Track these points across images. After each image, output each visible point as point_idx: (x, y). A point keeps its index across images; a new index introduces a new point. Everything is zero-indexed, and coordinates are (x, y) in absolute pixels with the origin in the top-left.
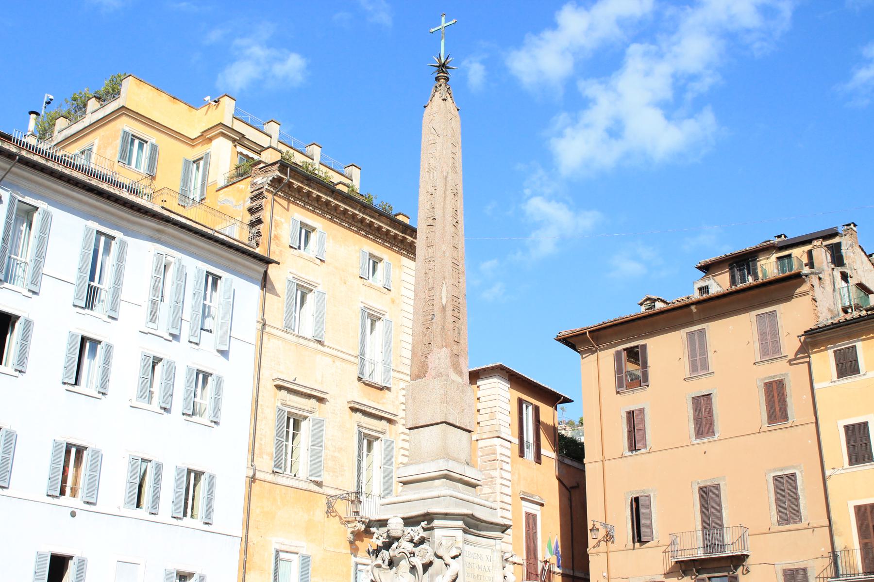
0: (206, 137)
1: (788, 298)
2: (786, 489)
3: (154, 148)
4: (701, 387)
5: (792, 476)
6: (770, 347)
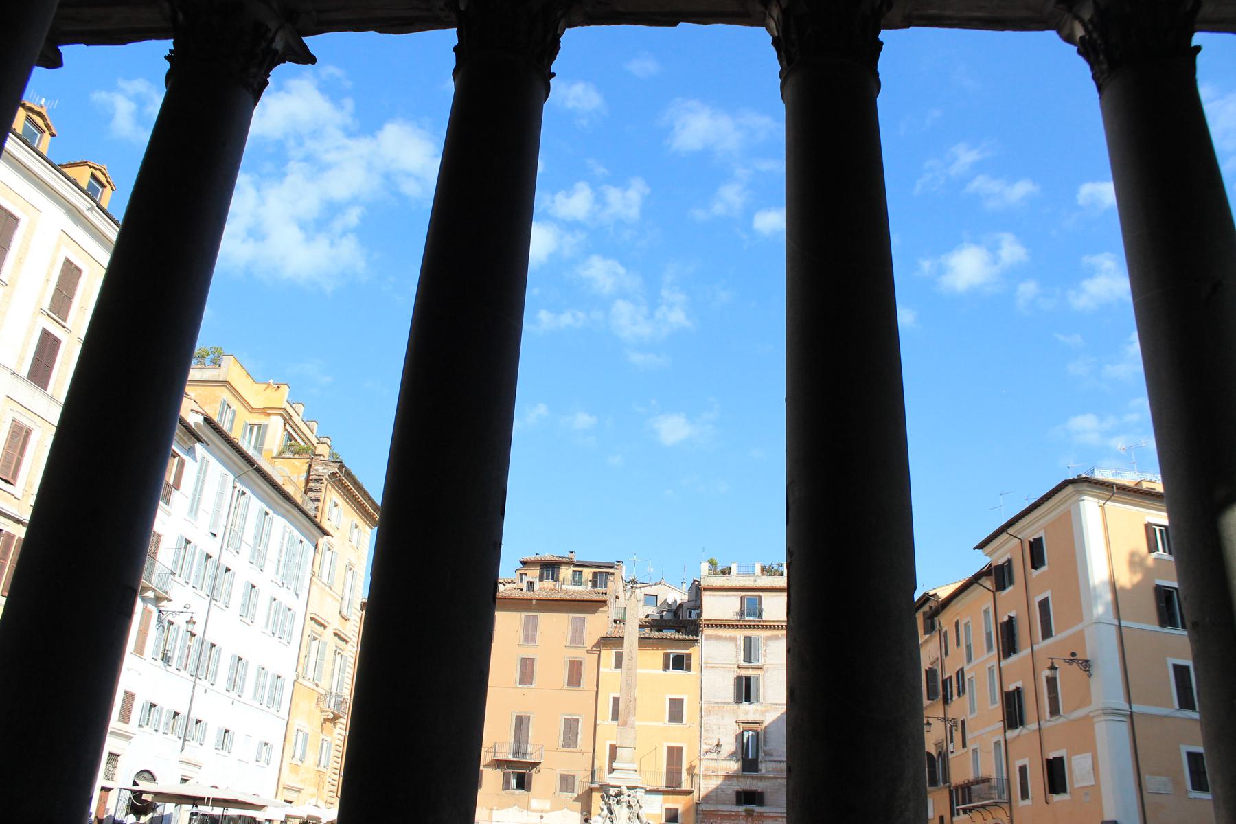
0: (265, 412)
1: (594, 612)
2: (571, 727)
3: (235, 412)
4: (528, 652)
5: (577, 720)
6: (577, 638)
